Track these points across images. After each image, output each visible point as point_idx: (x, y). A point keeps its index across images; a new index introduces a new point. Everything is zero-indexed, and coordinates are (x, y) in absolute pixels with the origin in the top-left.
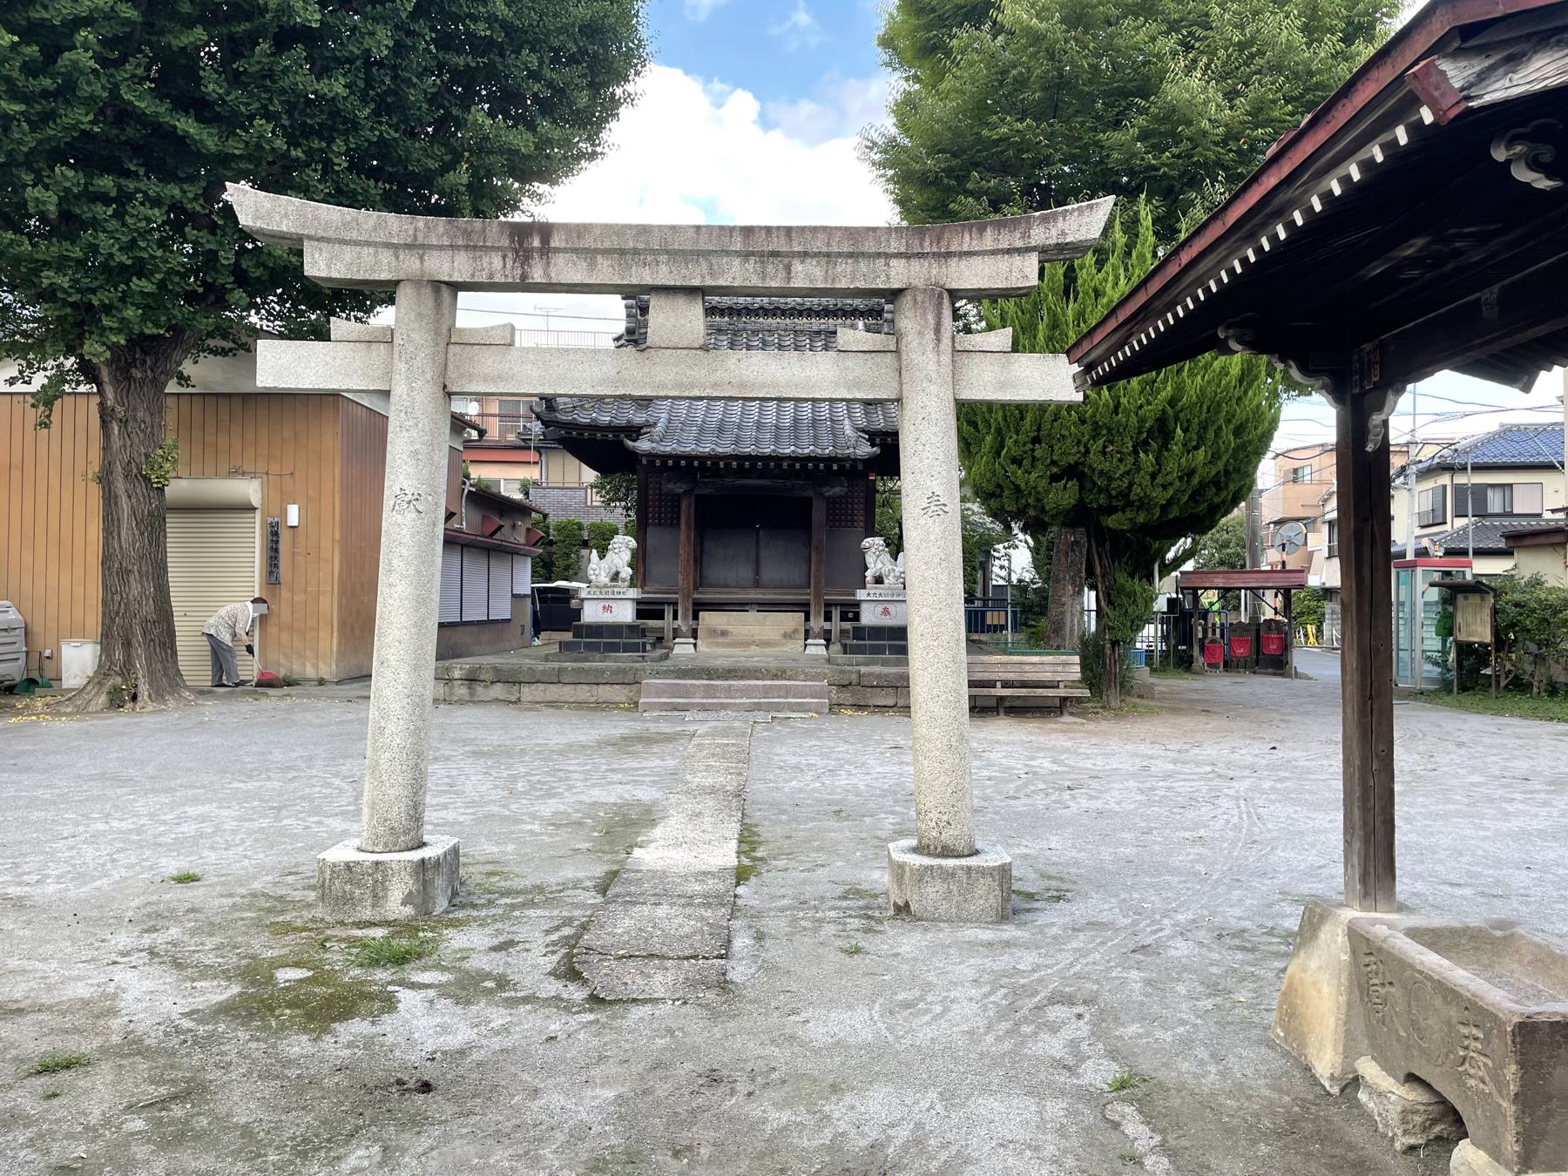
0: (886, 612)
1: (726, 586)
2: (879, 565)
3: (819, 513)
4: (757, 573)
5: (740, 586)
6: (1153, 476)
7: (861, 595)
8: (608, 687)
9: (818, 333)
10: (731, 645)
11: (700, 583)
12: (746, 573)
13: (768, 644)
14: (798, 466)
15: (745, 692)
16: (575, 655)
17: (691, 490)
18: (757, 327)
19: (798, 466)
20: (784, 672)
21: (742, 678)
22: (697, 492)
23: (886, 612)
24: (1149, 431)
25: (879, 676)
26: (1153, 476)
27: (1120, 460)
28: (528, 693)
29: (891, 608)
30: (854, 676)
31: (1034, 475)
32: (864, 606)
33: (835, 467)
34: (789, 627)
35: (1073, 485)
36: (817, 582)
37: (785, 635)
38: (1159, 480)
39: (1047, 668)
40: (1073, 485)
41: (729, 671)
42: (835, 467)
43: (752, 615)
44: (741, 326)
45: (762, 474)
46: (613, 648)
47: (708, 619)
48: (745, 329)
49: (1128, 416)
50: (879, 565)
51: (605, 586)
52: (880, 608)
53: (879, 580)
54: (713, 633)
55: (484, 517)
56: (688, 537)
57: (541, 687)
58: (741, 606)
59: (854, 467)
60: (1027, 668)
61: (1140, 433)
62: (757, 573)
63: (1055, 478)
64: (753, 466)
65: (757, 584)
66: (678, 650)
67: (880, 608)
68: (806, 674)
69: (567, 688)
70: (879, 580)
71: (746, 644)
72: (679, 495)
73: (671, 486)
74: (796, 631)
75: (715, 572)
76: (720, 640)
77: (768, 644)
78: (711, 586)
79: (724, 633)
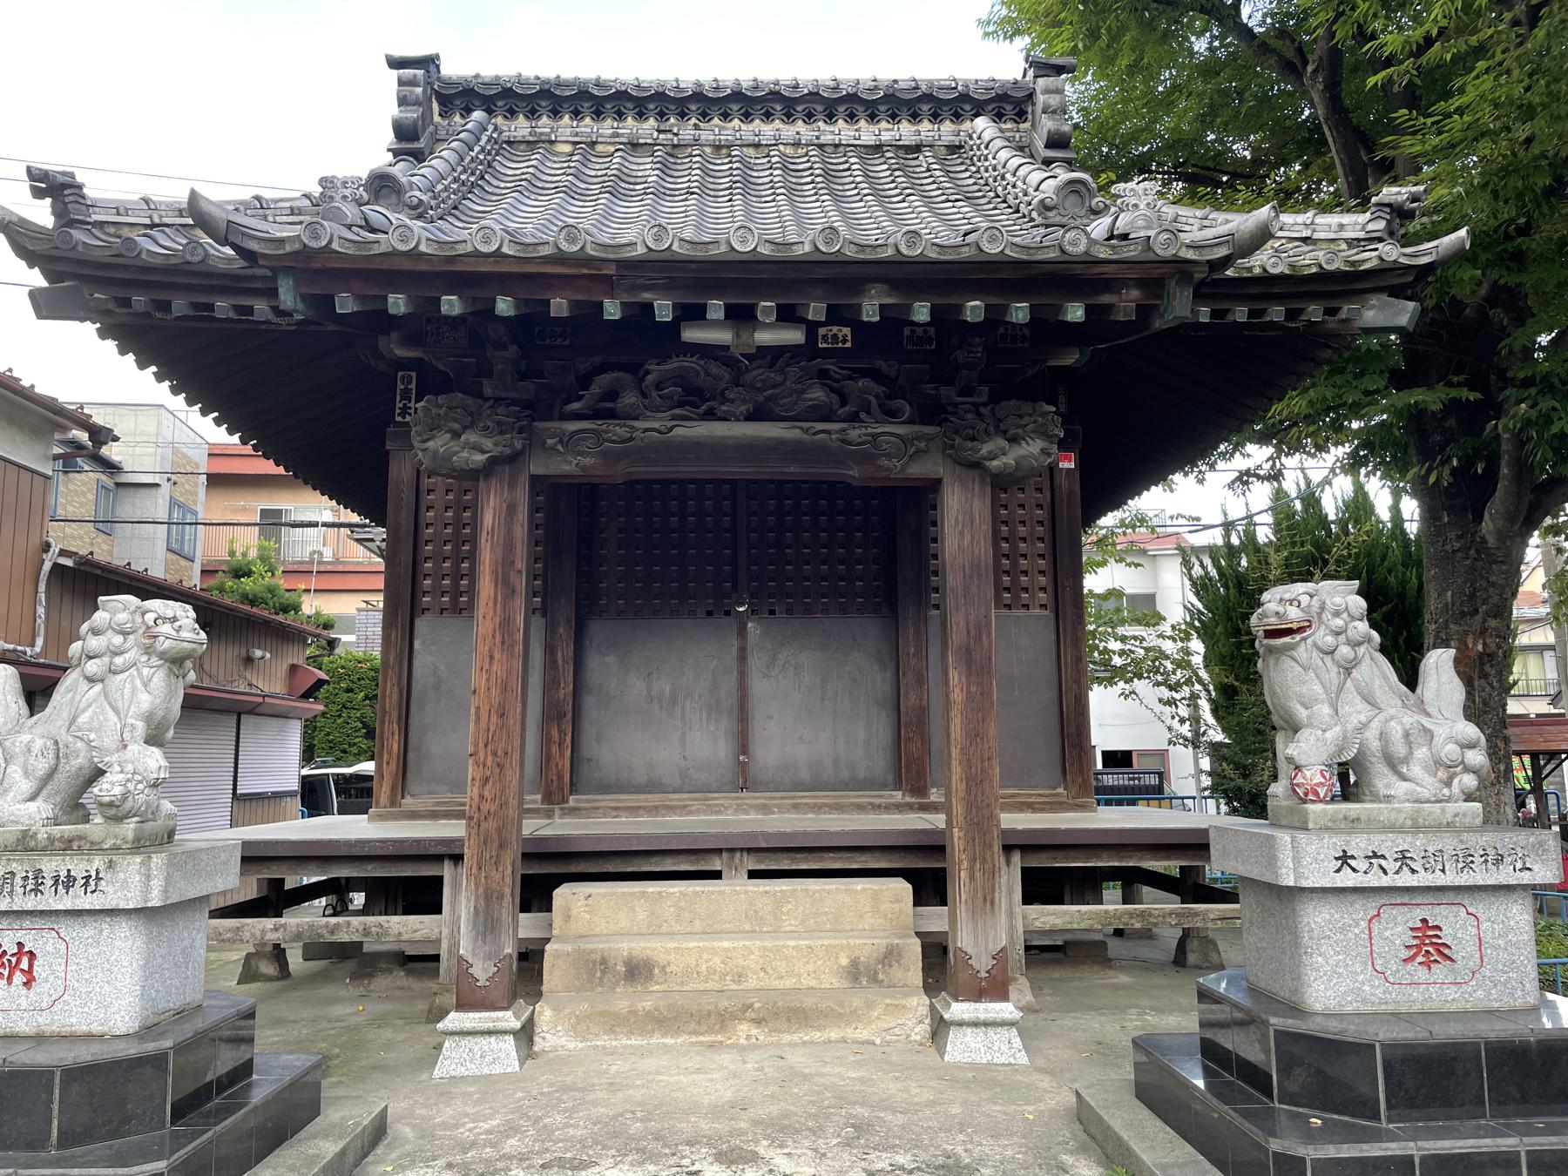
0: (1429, 946)
1: (653, 786)
4: (743, 744)
5: (694, 786)
7: (1304, 858)
9: (878, 148)
10: (664, 1021)
11: (566, 779)
12: (708, 744)
13: (788, 1012)
17: (513, 459)
22: (538, 467)
23: (1429, 946)
29: (1453, 924)
32: (1316, 917)
34: (868, 946)
36: (975, 781)
37: (855, 972)
43: (736, 892)
47: (581, 906)
50: (1355, 711)
52: (1397, 927)
53: (1349, 781)
54: (596, 969)
56: (506, 624)
58: (692, 862)
62: (743, 744)
65: (743, 779)
66: (455, 1060)
67: (1397, 927)
70: (1349, 781)
71: (710, 1017)
72: (472, 477)
73: (440, 443)
74: (891, 956)
76: (622, 1000)
77: (788, 1012)
78: (605, 788)
79: (637, 971)
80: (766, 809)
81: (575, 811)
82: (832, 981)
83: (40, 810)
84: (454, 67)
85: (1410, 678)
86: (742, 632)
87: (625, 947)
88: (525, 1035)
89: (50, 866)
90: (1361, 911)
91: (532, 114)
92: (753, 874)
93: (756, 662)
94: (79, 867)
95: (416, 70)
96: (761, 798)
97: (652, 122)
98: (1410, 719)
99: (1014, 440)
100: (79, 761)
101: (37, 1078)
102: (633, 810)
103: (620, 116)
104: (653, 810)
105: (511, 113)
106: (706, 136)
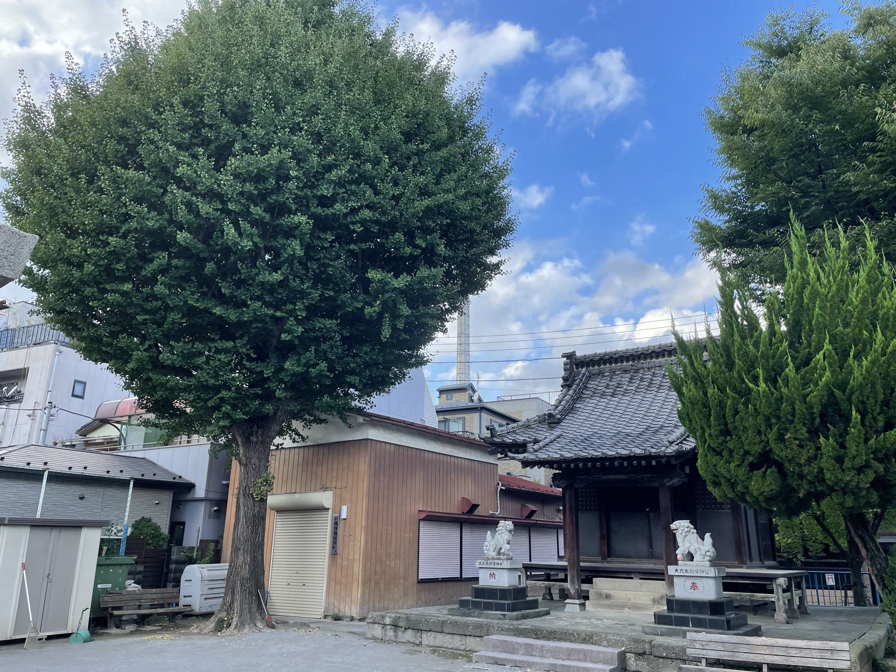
0: (694, 586)
2: (687, 545)
3: (665, 501)
5: (639, 557)
6: (840, 460)
8: (472, 639)
12: (643, 546)
13: (636, 607)
14: (625, 463)
15: (555, 653)
16: (466, 610)
18: (651, 365)
19: (625, 463)
20: (591, 637)
21: (560, 640)
23: (694, 586)
24: (822, 416)
25: (667, 648)
26: (840, 460)
27: (801, 446)
28: (428, 639)
29: (698, 582)
30: (647, 646)
31: (732, 465)
32: (675, 580)
33: (654, 463)
34: (657, 596)
35: (772, 471)
38: (847, 464)
39: (814, 654)
40: (772, 471)
41: (551, 633)
42: (654, 463)
43: (636, 582)
44: (640, 366)
45: (620, 470)
46: (488, 607)
47: (601, 584)
48: (642, 368)
49: (793, 405)
51: (493, 558)
52: (689, 582)
54: (600, 595)
55: (522, 505)
57: (433, 634)
58: (627, 574)
59: (668, 462)
60: (793, 652)
61: (813, 419)
62: (651, 547)
63: (753, 467)
64: (594, 465)
66: (568, 608)
67: (689, 582)
68: (608, 641)
69: (449, 637)
71: (622, 607)
75: (618, 545)
76: (606, 602)
79: (608, 597)
80: (655, 564)
81: (608, 562)
82: (650, 602)
83: (495, 553)
84: (579, 354)
85: (703, 540)
86: (649, 516)
87: (605, 591)
88: (583, 606)
89: (496, 561)
90: (684, 579)
91: (599, 365)
92: (642, 579)
93: (652, 524)
94: (500, 562)
95: (570, 356)
96: (654, 561)
97: (631, 363)
98: (697, 546)
99: (671, 479)
100: (498, 547)
101: (496, 590)
102: (622, 562)
103: (622, 362)
104: (627, 563)
105: (593, 366)
106: (645, 366)
